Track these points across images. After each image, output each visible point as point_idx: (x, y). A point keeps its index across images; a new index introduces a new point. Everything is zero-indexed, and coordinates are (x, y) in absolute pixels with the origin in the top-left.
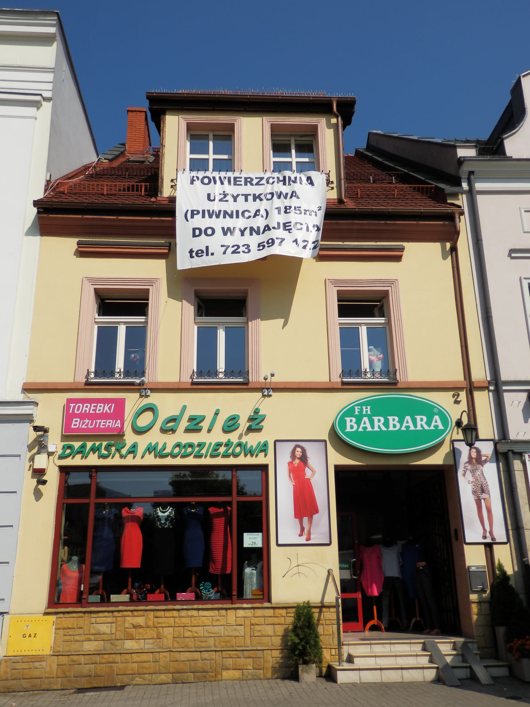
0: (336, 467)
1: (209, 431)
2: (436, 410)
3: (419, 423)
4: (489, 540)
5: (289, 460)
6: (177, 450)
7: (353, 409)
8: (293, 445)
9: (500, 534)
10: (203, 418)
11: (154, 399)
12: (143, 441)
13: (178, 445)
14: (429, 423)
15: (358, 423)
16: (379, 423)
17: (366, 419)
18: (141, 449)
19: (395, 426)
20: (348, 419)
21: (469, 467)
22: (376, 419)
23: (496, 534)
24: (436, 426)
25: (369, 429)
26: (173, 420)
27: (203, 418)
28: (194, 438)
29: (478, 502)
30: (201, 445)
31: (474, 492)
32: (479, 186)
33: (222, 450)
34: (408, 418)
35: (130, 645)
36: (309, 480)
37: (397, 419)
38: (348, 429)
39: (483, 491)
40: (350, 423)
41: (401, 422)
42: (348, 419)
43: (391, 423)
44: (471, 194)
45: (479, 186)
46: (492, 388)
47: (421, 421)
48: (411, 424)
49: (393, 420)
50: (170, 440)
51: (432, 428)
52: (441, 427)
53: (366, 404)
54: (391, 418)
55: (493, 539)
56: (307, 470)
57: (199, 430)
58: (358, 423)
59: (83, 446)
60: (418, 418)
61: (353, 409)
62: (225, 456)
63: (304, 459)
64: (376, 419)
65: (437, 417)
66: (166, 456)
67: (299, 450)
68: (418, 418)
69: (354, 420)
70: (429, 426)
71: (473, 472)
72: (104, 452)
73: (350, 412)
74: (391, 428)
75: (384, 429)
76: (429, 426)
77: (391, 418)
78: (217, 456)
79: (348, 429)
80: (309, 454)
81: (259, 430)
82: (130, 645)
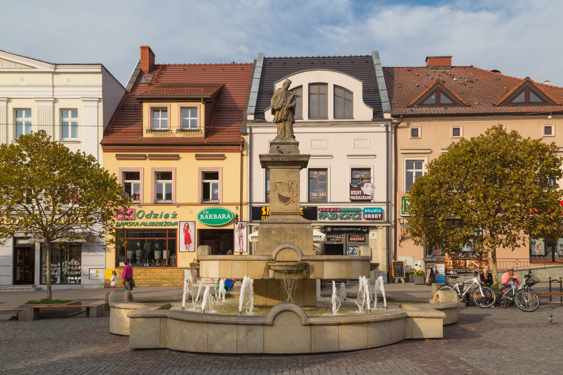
0: (198, 229)
1: (161, 217)
2: (229, 212)
3: (223, 216)
4: (241, 251)
5: (184, 227)
6: (150, 224)
7: (203, 212)
8: (184, 223)
9: (245, 249)
10: (158, 215)
11: (143, 208)
12: (140, 221)
13: (150, 223)
14: (226, 217)
15: (204, 217)
16: (211, 216)
17: (207, 215)
18: (140, 224)
19: (215, 217)
20: (201, 215)
21: (238, 230)
22: (210, 215)
23: (243, 249)
24: (228, 218)
25: (208, 218)
26: (149, 215)
27: (158, 215)
28: (155, 221)
29: (240, 240)
30: (158, 223)
31: (239, 237)
33: (164, 224)
34: (220, 215)
36: (189, 234)
37: (216, 215)
38: (201, 218)
39: (241, 237)
40: (202, 216)
41: (217, 216)
42: (201, 215)
43: (214, 216)
44: (251, 134)
45: (254, 130)
46: (248, 205)
47: (224, 216)
48: (220, 217)
49: (215, 216)
50: (148, 221)
51: (227, 218)
52: (230, 218)
53: (207, 210)
54: (214, 215)
55: (243, 251)
56: (189, 231)
57: (157, 218)
58: (204, 217)
59: (122, 223)
60: (223, 215)
61: (203, 212)
62: (165, 225)
63: (188, 227)
64: (210, 215)
65: (229, 215)
66: (148, 226)
67: (187, 224)
68: (223, 215)
69: (203, 215)
70: (226, 217)
71: (239, 231)
72: (129, 225)
73: (202, 213)
74: (214, 218)
75: (212, 218)
76: (226, 217)
77: (214, 215)
78: (163, 226)
79: (201, 218)
80: (189, 225)
81: (176, 218)
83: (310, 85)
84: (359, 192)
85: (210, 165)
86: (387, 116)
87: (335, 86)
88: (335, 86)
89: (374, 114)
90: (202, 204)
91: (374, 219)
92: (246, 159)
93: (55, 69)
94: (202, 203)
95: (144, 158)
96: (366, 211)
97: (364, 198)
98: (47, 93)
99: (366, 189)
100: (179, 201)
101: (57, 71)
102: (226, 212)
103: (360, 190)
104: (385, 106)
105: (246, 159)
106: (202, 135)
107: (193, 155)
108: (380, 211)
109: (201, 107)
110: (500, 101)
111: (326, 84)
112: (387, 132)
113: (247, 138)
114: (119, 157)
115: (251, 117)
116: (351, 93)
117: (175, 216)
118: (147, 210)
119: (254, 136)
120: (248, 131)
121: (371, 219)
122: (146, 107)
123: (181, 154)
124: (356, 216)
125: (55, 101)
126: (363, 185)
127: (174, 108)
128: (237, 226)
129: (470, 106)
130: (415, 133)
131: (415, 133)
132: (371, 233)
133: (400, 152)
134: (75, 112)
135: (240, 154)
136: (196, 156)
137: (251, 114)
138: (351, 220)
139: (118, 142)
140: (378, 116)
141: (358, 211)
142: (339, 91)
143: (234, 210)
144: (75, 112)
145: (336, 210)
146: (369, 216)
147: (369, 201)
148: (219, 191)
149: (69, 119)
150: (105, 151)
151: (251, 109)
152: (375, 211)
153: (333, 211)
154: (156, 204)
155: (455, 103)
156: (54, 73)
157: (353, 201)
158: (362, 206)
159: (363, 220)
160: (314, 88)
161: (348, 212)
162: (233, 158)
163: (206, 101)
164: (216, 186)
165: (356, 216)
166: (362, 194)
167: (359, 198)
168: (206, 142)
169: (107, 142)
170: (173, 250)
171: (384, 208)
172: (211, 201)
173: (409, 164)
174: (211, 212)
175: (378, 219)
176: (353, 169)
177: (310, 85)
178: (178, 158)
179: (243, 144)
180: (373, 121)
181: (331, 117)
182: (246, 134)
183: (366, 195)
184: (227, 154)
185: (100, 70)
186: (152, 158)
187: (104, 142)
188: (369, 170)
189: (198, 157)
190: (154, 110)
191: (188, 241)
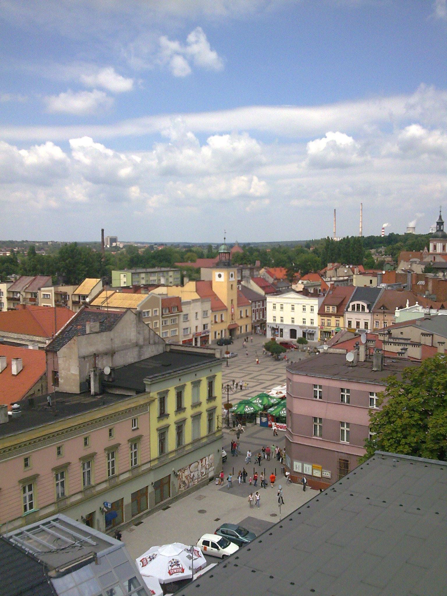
86: (371, 312)
90: (336, 327)
95: (325, 317)
100: (332, 326)
106: (336, 313)
114: (321, 316)
115: (345, 310)
117: (331, 329)
118: (326, 327)
127: (331, 307)
140: (370, 312)
151: (346, 308)
154: (327, 326)
162: (341, 318)
163: (337, 306)
186: (327, 317)
189: (335, 317)
190: (328, 307)
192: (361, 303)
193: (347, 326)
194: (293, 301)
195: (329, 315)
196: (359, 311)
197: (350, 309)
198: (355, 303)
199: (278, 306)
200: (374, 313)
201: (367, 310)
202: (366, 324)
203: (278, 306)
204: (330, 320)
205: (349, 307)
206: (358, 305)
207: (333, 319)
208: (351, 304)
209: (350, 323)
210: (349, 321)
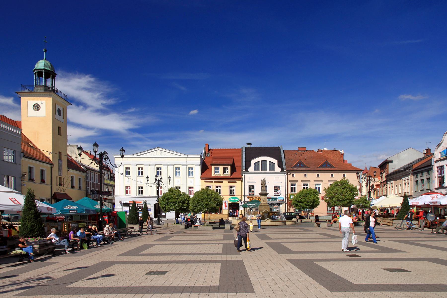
16: (232, 199)
32: (245, 174)
35: (211, 217)
44: (244, 175)
49: (234, 199)
63: (226, 202)
82: (211, 217)
83: (262, 161)
84: (277, 193)
85: (232, 184)
86: (285, 170)
87: (269, 161)
88: (269, 161)
89: (281, 170)
91: (281, 201)
92: (243, 183)
93: (187, 156)
94: (230, 195)
96: (279, 198)
97: (278, 194)
98: (185, 163)
99: (278, 192)
101: (188, 157)
102: (237, 198)
103: (277, 192)
104: (284, 167)
105: (243, 183)
106: (230, 175)
107: (227, 181)
108: (283, 198)
109: (229, 167)
110: (318, 166)
111: (267, 161)
112: (285, 175)
113: (243, 177)
114: (205, 182)
115: (244, 170)
116: (274, 164)
119: (245, 176)
120: (243, 174)
121: (280, 201)
122: (213, 167)
123: (223, 181)
124: (276, 200)
125: (187, 166)
126: (278, 191)
127: (221, 168)
128: (240, 202)
129: (309, 168)
130: (293, 175)
131: (293, 175)
132: (280, 205)
133: (288, 181)
134: (192, 169)
135: (241, 181)
136: (228, 181)
137: (244, 169)
138: (274, 201)
139: (205, 177)
140: (282, 170)
141: (277, 198)
142: (270, 163)
143: (240, 198)
144: (192, 169)
145: (270, 198)
146: (280, 200)
147: (280, 195)
148: (235, 192)
149: (191, 170)
150: (201, 180)
151: (244, 168)
152: (282, 198)
153: (269, 198)
155: (305, 166)
156: (187, 157)
157: (275, 195)
158: (277, 197)
159: (278, 201)
160: (262, 162)
161: (274, 199)
162: (239, 182)
164: (233, 190)
165: (276, 200)
166: (278, 193)
167: (277, 194)
168: (231, 178)
169: (202, 177)
170: (221, 209)
171: (284, 198)
172: (232, 194)
173: (292, 185)
174: (233, 198)
175: (282, 201)
176: (275, 186)
177: (262, 161)
178: (222, 182)
179: (242, 178)
180: (281, 172)
181: (268, 171)
182: (243, 175)
183: (279, 194)
184: (237, 181)
185: (200, 156)
186: (215, 182)
187: (201, 177)
188: (280, 186)
189: (229, 182)
190: (215, 168)
191: (226, 206)
192: (269, 159)
193: (247, 193)
194: (159, 162)
195: (219, 179)
196: (266, 170)
197: (251, 169)
198: (260, 159)
199: (134, 171)
200: (288, 172)
201: (277, 169)
202: (277, 189)
203: (134, 171)
204: (220, 187)
205: (248, 165)
206: (264, 162)
207: (225, 186)
208: (253, 162)
209: (251, 188)
210: (250, 186)
